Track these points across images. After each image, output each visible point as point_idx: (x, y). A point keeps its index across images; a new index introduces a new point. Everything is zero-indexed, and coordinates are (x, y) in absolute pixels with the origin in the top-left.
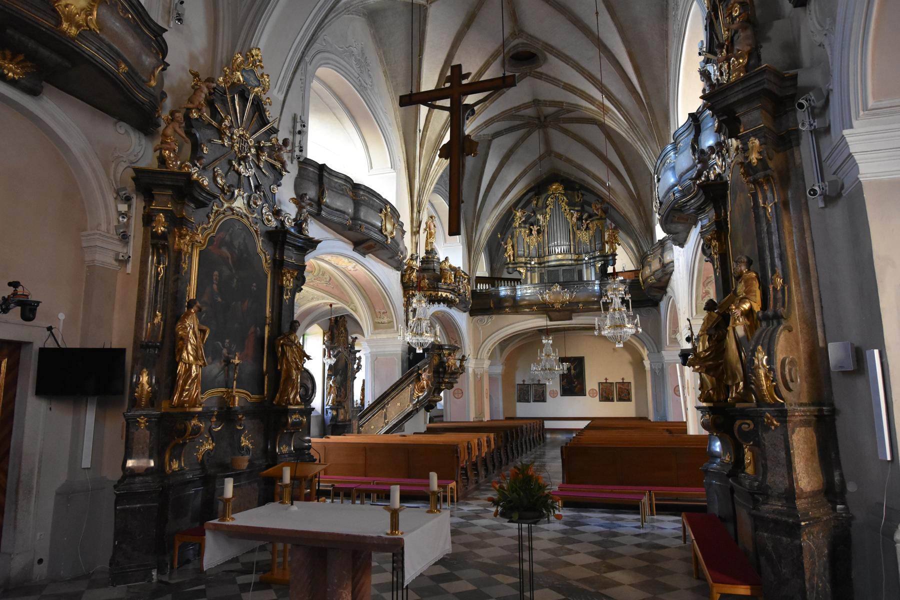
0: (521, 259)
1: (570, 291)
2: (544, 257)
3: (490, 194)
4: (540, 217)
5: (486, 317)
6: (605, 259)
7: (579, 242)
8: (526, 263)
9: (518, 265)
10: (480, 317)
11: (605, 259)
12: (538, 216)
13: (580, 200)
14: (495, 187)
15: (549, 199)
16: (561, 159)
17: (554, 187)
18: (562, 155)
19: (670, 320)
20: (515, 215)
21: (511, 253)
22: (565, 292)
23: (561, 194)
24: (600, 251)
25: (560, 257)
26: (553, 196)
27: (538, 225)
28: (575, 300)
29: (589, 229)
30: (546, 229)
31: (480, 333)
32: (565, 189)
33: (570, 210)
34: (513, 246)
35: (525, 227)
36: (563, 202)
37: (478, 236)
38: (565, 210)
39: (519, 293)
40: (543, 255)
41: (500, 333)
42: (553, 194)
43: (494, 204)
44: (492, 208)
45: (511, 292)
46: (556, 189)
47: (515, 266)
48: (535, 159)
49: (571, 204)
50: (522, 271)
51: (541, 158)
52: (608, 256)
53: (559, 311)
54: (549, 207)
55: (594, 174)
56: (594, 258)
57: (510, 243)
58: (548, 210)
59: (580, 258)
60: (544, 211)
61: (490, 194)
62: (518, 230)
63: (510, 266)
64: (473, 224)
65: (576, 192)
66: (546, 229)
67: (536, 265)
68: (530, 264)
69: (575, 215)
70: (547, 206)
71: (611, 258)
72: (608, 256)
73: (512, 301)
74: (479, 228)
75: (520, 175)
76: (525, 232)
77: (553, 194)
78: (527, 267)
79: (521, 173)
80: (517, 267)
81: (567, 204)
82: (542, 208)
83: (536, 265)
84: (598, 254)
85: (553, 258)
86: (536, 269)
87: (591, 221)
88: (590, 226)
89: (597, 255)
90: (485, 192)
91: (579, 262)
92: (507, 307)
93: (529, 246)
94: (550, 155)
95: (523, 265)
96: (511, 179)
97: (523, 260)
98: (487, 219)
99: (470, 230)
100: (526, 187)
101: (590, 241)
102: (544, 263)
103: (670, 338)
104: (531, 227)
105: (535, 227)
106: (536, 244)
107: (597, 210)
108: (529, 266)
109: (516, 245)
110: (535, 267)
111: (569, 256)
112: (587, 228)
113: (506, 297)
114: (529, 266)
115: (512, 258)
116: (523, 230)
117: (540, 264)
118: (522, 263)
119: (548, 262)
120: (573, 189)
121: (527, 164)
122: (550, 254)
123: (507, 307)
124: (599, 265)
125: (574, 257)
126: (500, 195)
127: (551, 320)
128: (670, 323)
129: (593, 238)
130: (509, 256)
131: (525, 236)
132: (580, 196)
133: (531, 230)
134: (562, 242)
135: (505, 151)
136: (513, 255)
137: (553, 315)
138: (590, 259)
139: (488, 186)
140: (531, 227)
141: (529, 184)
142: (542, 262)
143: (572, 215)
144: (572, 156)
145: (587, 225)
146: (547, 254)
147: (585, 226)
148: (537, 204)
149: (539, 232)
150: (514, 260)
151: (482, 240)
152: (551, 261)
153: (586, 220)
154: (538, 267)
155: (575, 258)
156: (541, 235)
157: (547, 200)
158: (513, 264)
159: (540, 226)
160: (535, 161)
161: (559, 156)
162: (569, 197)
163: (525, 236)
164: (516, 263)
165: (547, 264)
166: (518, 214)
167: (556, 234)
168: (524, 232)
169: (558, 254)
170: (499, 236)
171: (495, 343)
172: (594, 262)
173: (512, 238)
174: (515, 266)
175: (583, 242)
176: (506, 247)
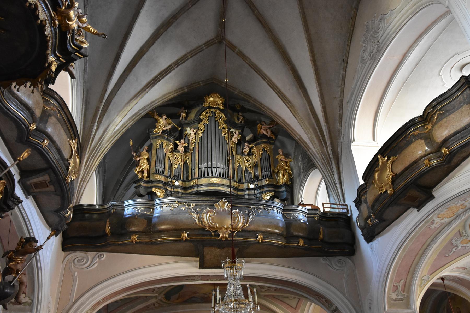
0: (159, 176)
1: (244, 213)
2: (192, 180)
3: (130, 74)
4: (189, 131)
5: (91, 255)
6: (276, 190)
7: (240, 168)
8: (165, 184)
9: (155, 184)
10: (80, 254)
11: (276, 190)
12: (188, 129)
13: (241, 122)
14: (139, 68)
15: (204, 113)
16: (234, 51)
17: (211, 99)
18: (236, 47)
19: (397, 262)
20: (157, 121)
21: (145, 166)
22: (238, 213)
23: (220, 110)
24: (268, 179)
25: (215, 180)
26: (208, 110)
27: (187, 140)
28: (252, 228)
29: (253, 154)
30: (197, 146)
31: (74, 280)
32: (224, 104)
33: (229, 130)
34: (148, 160)
35: (169, 141)
36: (220, 118)
37: (101, 131)
38: (224, 128)
39: (158, 211)
40: (190, 179)
41: (115, 283)
42: (210, 107)
43: (133, 92)
44: (130, 97)
45: (146, 209)
46: (214, 101)
47: (149, 185)
48: (200, 44)
49: (230, 123)
50: (159, 194)
51: (208, 44)
52: (280, 187)
53: (221, 244)
54: (204, 121)
55: (270, 79)
56: (262, 187)
57: (145, 154)
58: (201, 126)
59: (240, 188)
60: (196, 125)
61: (131, 77)
62: (159, 141)
63: (142, 184)
64: (98, 108)
65: (235, 114)
66: (197, 146)
67: (180, 190)
68: (173, 186)
69: (236, 136)
70: (200, 120)
71: (284, 189)
72: (280, 187)
73: (146, 222)
74: (105, 122)
75: (176, 61)
76: (168, 145)
77: (210, 107)
78: (166, 190)
79: (178, 60)
80: (152, 187)
81: (225, 122)
82: (194, 122)
83: (180, 190)
84: (266, 182)
85: (204, 181)
86: (180, 195)
87: (255, 145)
88: (255, 150)
89: (264, 184)
90: (124, 71)
91: (239, 193)
92: (135, 232)
93: (171, 165)
94: (220, 42)
95: (161, 185)
96: (164, 65)
97: (161, 178)
98: (120, 111)
99: (90, 117)
100: (178, 90)
101: (255, 169)
102: (191, 187)
103: (389, 298)
104: (177, 142)
105: (182, 141)
106: (181, 163)
107: (266, 131)
108: (169, 189)
109: (153, 160)
110: (178, 192)
111: (226, 182)
112: (250, 154)
113: (133, 216)
114: (169, 189)
115: (145, 174)
116: (165, 143)
117: (185, 189)
118: (160, 182)
119: (198, 186)
120: (234, 109)
121: (189, 50)
122: (200, 177)
123: (135, 232)
124: (268, 198)
125: (235, 185)
126: (144, 83)
127: (202, 266)
128: (394, 271)
129: (259, 164)
130: (142, 172)
131: (167, 150)
132: (241, 118)
133: (176, 146)
134: (218, 164)
135: (166, 14)
136: (149, 172)
137: (210, 252)
138: (255, 189)
139: (130, 63)
140: (177, 142)
141: (182, 88)
142: (187, 186)
143: (232, 134)
144: (247, 52)
145: (251, 149)
146: (197, 175)
147: (247, 149)
148: (186, 118)
149: (186, 149)
150: (148, 177)
151: (106, 139)
152: (202, 185)
153: (250, 142)
154: (182, 194)
155: (235, 186)
156: (188, 154)
157: (200, 115)
158: (147, 182)
159: (189, 144)
160: (200, 46)
161: (233, 47)
162: (229, 116)
163: (167, 150)
164: (152, 182)
165: (195, 189)
166: (162, 121)
167: (210, 153)
168: (167, 145)
169: (213, 177)
170: (131, 143)
171: (99, 303)
172: (261, 193)
173: (149, 150)
174: (149, 185)
175: (244, 169)
176: (138, 159)
